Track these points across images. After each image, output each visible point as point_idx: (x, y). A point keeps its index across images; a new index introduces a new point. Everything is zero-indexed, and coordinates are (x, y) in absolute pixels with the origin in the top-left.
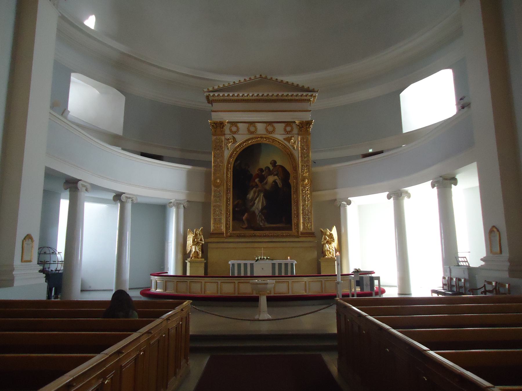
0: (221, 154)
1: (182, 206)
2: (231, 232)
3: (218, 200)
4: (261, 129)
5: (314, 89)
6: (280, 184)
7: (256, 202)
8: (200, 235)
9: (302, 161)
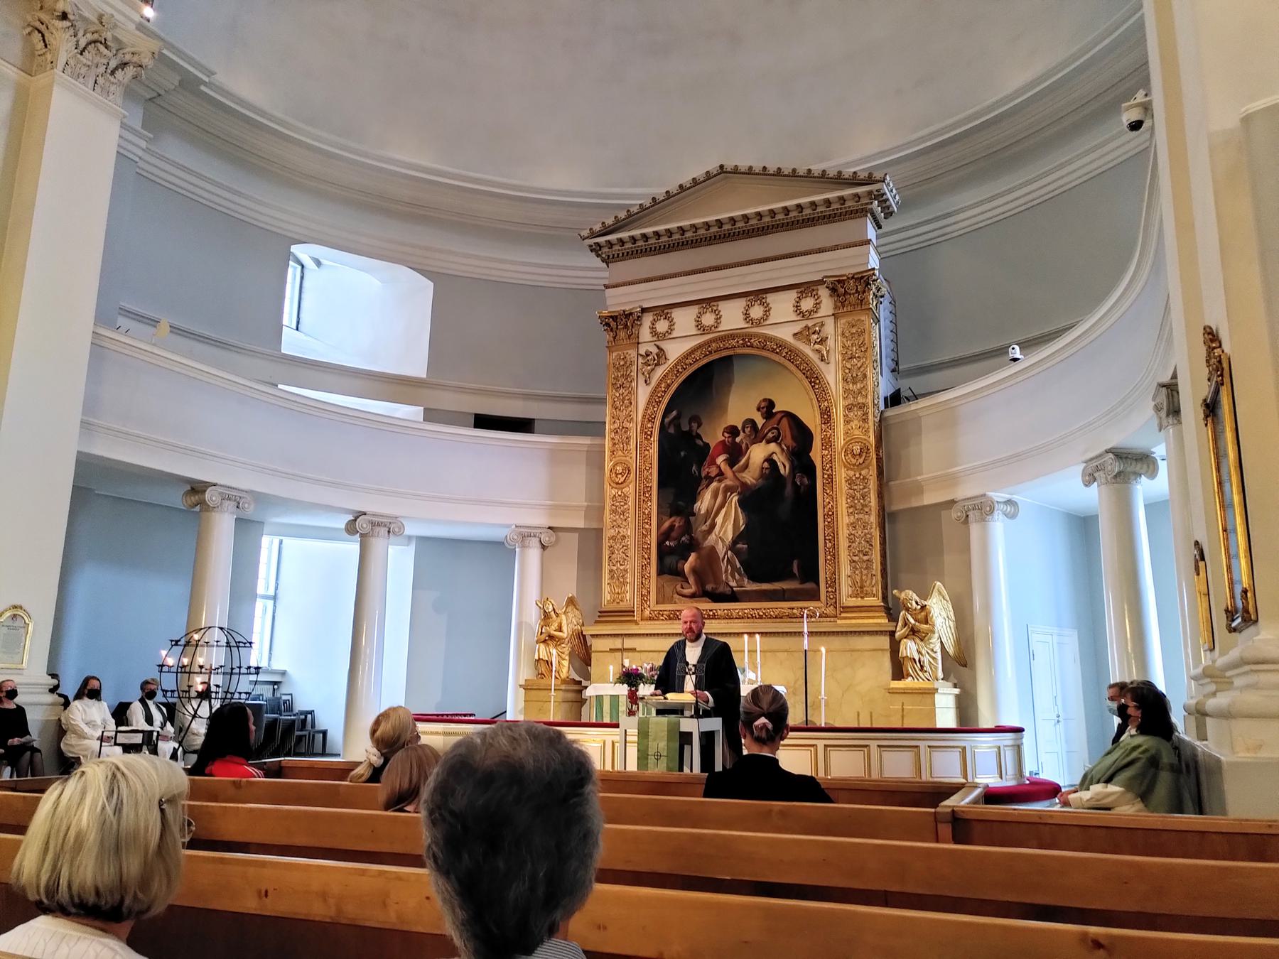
0: (627, 398)
1: (534, 542)
2: (652, 606)
3: (619, 522)
4: (732, 317)
5: (870, 175)
6: (785, 467)
7: (719, 520)
8: (557, 615)
9: (846, 391)
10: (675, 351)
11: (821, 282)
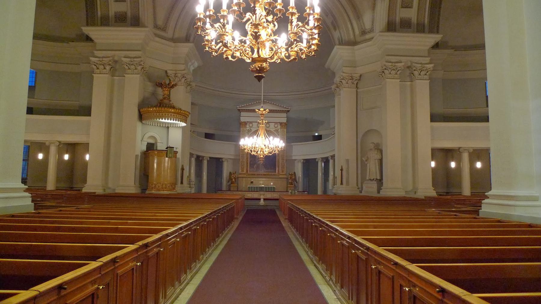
11: (279, 122)
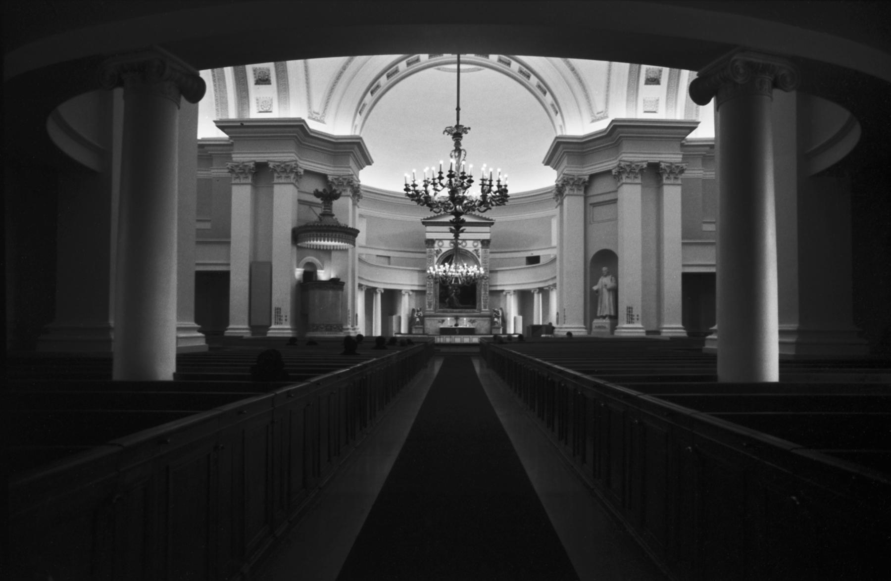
1: (407, 294)
10: (444, 250)
11: (479, 240)
